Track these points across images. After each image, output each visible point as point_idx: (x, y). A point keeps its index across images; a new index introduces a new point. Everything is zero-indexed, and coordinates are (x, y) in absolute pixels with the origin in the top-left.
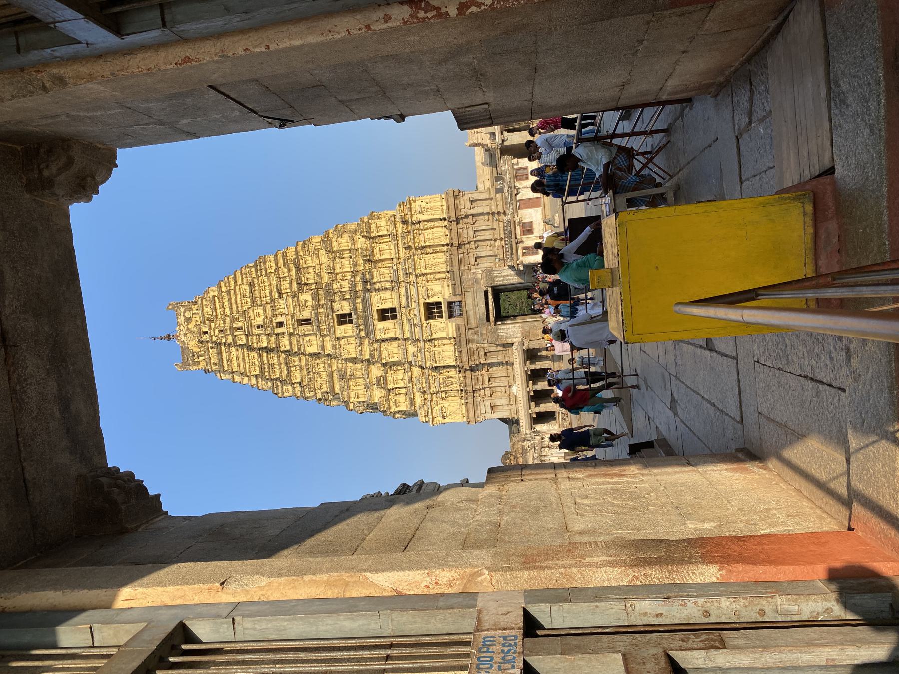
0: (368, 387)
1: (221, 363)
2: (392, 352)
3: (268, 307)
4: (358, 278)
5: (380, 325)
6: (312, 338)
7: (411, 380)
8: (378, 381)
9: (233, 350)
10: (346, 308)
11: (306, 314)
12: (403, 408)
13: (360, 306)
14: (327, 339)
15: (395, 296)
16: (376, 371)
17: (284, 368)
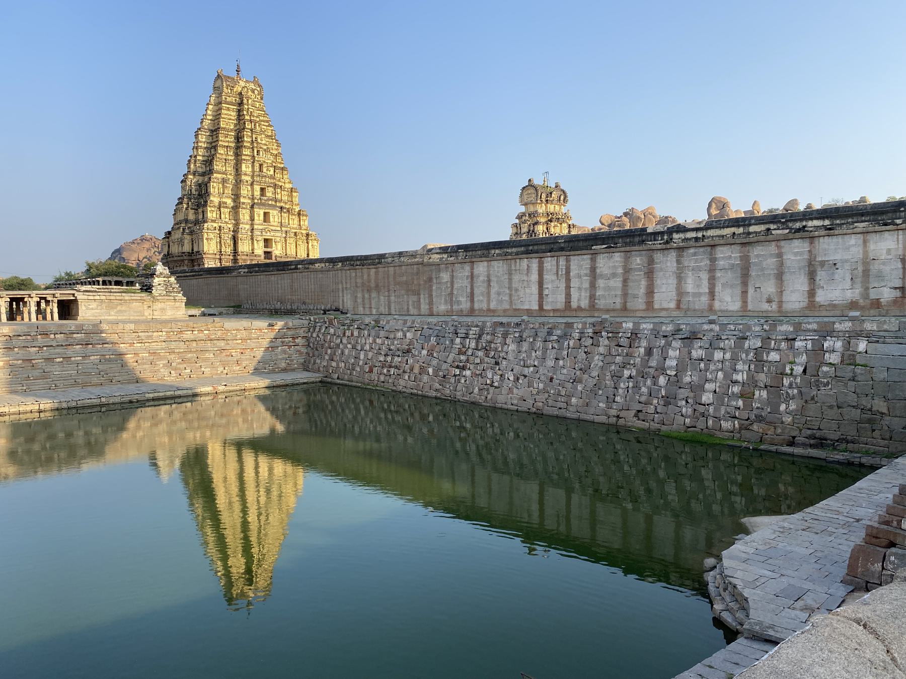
0: (221, 195)
1: (227, 103)
2: (244, 215)
3: (265, 147)
4: (282, 204)
5: (262, 212)
6: (250, 169)
7: (226, 223)
8: (226, 203)
9: (234, 114)
10: (269, 193)
11: (265, 170)
12: (209, 215)
13: (270, 202)
14: (248, 178)
15: (276, 224)
16: (230, 202)
17: (226, 144)
